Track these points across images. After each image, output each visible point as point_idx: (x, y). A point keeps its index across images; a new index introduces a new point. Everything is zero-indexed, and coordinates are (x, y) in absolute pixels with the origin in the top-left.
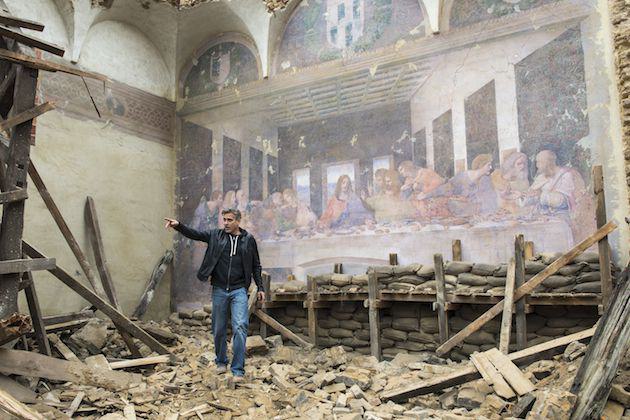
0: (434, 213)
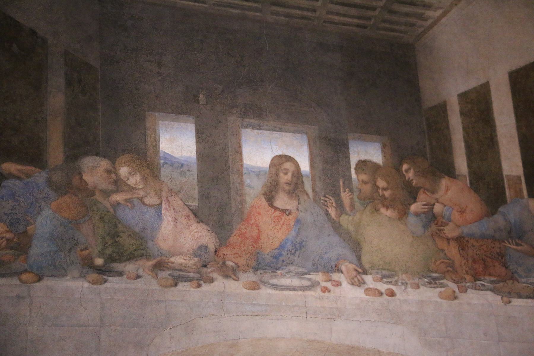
0: (480, 268)
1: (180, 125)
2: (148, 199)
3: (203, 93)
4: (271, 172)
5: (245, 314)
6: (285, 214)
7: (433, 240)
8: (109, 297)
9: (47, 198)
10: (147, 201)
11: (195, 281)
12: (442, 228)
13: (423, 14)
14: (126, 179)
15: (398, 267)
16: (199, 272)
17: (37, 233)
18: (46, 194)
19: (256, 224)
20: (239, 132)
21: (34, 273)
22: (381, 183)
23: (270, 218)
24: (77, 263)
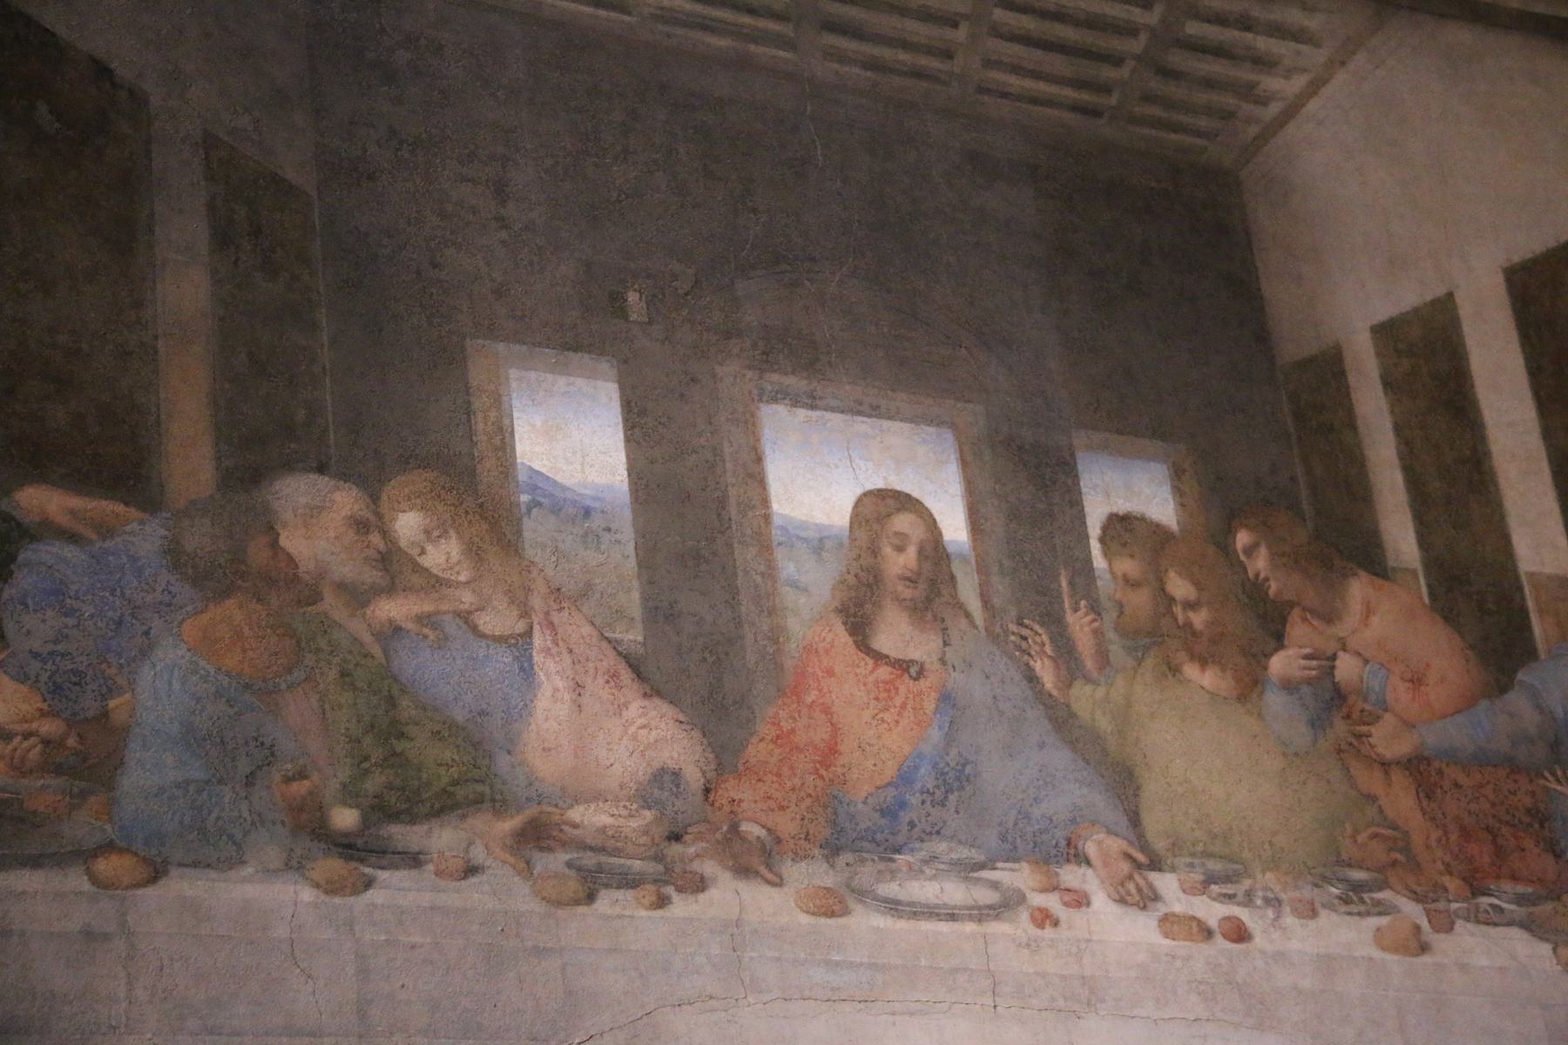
0: (1482, 854)
1: (573, 384)
2: (488, 618)
3: (636, 286)
4: (857, 543)
5: (807, 993)
6: (906, 675)
7: (1343, 764)
8: (383, 938)
9: (169, 605)
10: (487, 622)
11: (648, 886)
12: (1364, 729)
13: (1252, 86)
14: (414, 552)
15: (1250, 850)
16: (659, 858)
17: (140, 721)
18: (166, 592)
19: (823, 704)
20: (753, 416)
21: (136, 854)
22: (1180, 588)
23: (863, 688)
24: (274, 823)
